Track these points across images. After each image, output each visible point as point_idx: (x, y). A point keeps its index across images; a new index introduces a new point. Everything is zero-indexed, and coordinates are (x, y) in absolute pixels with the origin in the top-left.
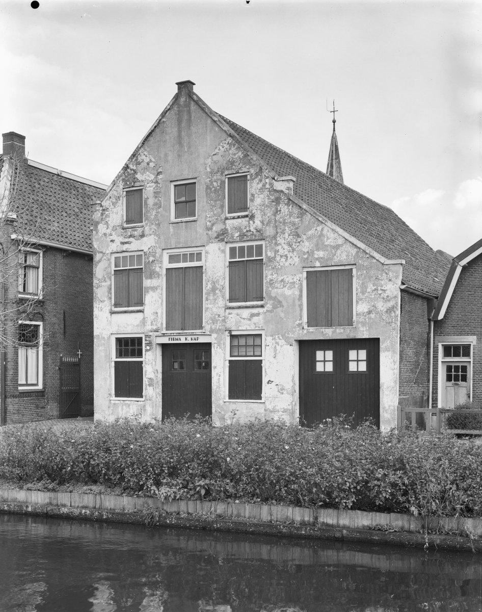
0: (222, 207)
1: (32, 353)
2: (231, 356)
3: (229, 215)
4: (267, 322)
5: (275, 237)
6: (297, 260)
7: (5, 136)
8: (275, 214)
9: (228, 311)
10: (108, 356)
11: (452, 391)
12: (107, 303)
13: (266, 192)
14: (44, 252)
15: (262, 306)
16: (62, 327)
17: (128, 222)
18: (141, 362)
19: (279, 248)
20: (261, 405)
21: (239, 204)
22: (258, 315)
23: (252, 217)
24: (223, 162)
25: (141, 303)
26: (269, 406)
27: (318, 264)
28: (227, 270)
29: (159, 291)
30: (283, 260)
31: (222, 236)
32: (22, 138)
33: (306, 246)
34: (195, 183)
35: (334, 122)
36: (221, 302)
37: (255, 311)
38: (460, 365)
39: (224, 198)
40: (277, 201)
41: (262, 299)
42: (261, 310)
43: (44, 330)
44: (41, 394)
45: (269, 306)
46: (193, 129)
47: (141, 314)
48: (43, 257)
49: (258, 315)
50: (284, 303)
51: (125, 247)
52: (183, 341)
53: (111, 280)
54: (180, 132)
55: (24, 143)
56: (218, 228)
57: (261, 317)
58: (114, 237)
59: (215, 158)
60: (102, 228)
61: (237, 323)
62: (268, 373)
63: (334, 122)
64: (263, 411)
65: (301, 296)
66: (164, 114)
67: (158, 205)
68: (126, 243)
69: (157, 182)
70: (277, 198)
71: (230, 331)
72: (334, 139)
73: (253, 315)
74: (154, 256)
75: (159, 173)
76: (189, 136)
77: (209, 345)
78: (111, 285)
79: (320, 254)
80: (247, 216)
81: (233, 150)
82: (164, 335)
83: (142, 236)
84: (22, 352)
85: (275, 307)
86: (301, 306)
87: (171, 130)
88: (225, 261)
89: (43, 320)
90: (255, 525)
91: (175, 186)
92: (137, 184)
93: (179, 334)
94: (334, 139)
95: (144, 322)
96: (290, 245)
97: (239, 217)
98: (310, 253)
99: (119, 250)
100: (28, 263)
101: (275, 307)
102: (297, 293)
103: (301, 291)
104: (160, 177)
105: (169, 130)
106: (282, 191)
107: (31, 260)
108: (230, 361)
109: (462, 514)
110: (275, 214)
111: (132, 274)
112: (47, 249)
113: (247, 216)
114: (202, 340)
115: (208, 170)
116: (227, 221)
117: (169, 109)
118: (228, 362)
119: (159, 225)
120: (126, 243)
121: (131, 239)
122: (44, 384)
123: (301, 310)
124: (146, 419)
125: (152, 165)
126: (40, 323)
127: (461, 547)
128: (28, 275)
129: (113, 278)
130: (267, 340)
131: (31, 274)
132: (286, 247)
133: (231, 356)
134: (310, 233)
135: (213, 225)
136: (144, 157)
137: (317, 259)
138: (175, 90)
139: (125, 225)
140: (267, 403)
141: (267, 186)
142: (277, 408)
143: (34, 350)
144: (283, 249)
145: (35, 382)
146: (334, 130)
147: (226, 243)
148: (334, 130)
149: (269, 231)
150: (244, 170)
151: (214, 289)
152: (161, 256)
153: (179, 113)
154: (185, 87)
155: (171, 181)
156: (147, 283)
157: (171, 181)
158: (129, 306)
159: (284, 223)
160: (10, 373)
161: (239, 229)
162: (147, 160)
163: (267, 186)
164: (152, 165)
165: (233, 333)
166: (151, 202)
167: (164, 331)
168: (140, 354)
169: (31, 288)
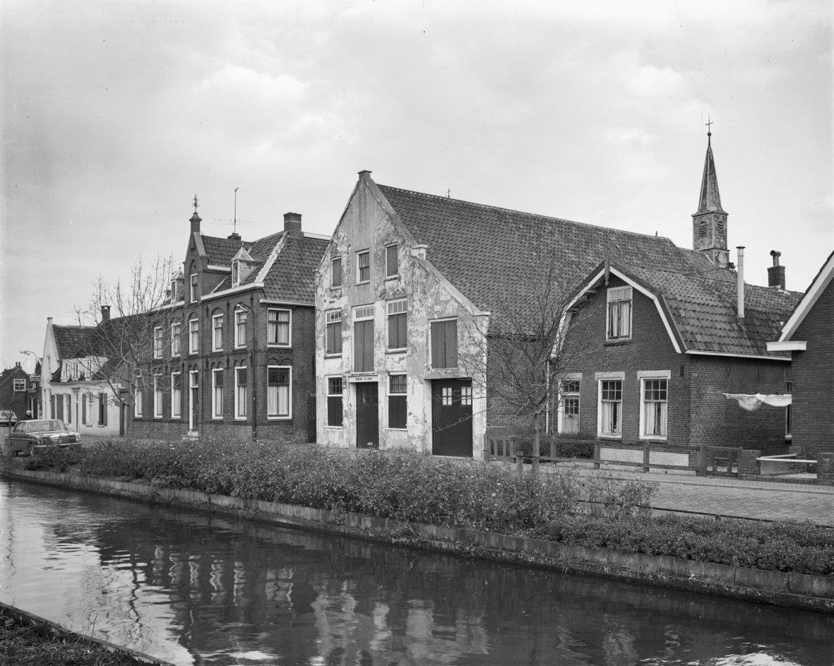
0: (383, 271)
1: (283, 390)
2: (391, 393)
3: (388, 278)
4: (408, 365)
5: (412, 295)
6: (425, 313)
7: (285, 216)
8: (412, 276)
9: (387, 356)
10: (323, 393)
11: (568, 421)
12: (323, 350)
13: (407, 259)
14: (293, 310)
15: (405, 352)
16: (312, 369)
17: (334, 285)
18: (341, 398)
19: (415, 303)
20: (406, 433)
21: (393, 269)
22: (403, 359)
23: (399, 279)
24: (383, 235)
25: (340, 351)
26: (410, 434)
27: (436, 317)
28: (387, 322)
29: (350, 340)
30: (417, 313)
31: (383, 295)
32: (298, 217)
33: (430, 301)
34: (368, 253)
35: (709, 134)
36: (383, 349)
37: (402, 355)
38: (574, 398)
39: (385, 263)
40: (413, 265)
41: (405, 345)
42: (404, 355)
43: (293, 371)
44: (289, 423)
45: (409, 352)
46: (368, 209)
47: (340, 359)
48: (292, 314)
49: (403, 359)
50: (418, 349)
51: (332, 306)
52: (363, 381)
53: (325, 332)
54: (360, 211)
55: (300, 220)
56: (380, 289)
57: (405, 360)
58: (326, 298)
59: (380, 231)
60: (319, 290)
61: (392, 365)
62: (411, 408)
63: (709, 134)
64: (406, 438)
65: (427, 343)
66: (352, 197)
67: (349, 271)
68: (332, 302)
69: (348, 253)
70: (414, 262)
71: (389, 372)
72: (709, 153)
73: (401, 359)
74: (347, 312)
75: (349, 246)
76: (365, 215)
77: (376, 383)
78: (325, 336)
79: (437, 308)
80: (395, 279)
81: (389, 225)
82: (353, 376)
83: (341, 296)
84: (272, 391)
85: (413, 353)
86: (427, 351)
87: (355, 210)
88: (385, 315)
89: (292, 364)
90: (186, 504)
91: (360, 255)
92: (338, 255)
93: (361, 375)
94: (709, 153)
95: (342, 365)
96: (420, 301)
97: (391, 280)
98: (432, 307)
99: (329, 308)
100: (279, 320)
101: (413, 353)
102: (425, 340)
103: (427, 339)
104: (350, 248)
105: (354, 210)
106: (416, 257)
107: (283, 318)
108: (390, 397)
109: (258, 499)
110: (412, 276)
111: (367, 324)
112: (295, 308)
113: (395, 279)
114: (374, 380)
115: (376, 241)
116: (387, 283)
117: (354, 194)
118: (388, 398)
119: (349, 287)
120: (332, 302)
121: (335, 299)
122: (293, 415)
123: (427, 355)
124: (343, 443)
125: (346, 239)
126: (290, 367)
127: (267, 521)
128: (279, 329)
129: (326, 330)
130: (409, 380)
131: (282, 329)
132: (418, 302)
133: (391, 393)
134: (432, 290)
135: (378, 286)
136: (341, 234)
137: (436, 312)
138: (357, 178)
139: (333, 288)
140: (409, 432)
141: (408, 253)
142: (415, 435)
143: (285, 388)
144: (417, 305)
145: (285, 413)
146: (709, 144)
147: (386, 300)
148: (709, 144)
149: (409, 291)
150: (395, 241)
151: (379, 339)
152: (351, 311)
153: (360, 198)
154: (364, 175)
155: (356, 252)
156: (344, 334)
157: (356, 252)
158: (335, 353)
159: (418, 283)
160: (260, 407)
161: (392, 289)
162: (343, 236)
163: (408, 253)
164: (346, 239)
165: (391, 374)
166: (345, 269)
167: (354, 373)
168: (341, 392)
169: (282, 339)
